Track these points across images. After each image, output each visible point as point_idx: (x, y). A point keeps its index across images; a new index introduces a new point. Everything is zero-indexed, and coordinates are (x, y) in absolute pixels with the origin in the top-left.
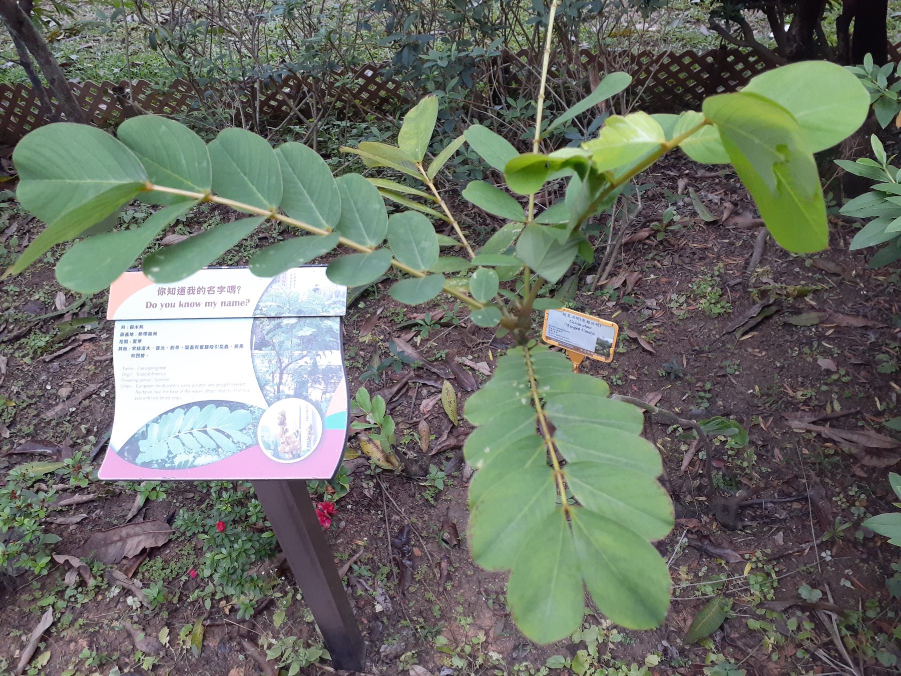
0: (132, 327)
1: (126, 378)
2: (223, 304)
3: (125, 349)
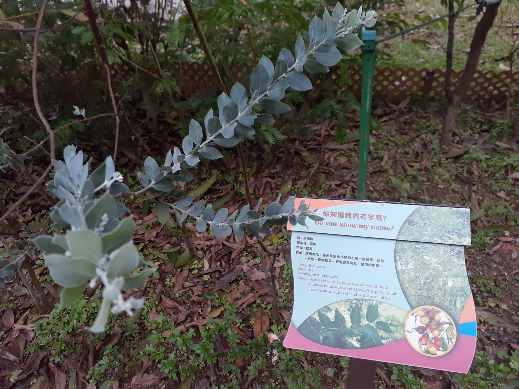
0: (305, 238)
1: (301, 271)
2: (373, 227)
3: (301, 253)
